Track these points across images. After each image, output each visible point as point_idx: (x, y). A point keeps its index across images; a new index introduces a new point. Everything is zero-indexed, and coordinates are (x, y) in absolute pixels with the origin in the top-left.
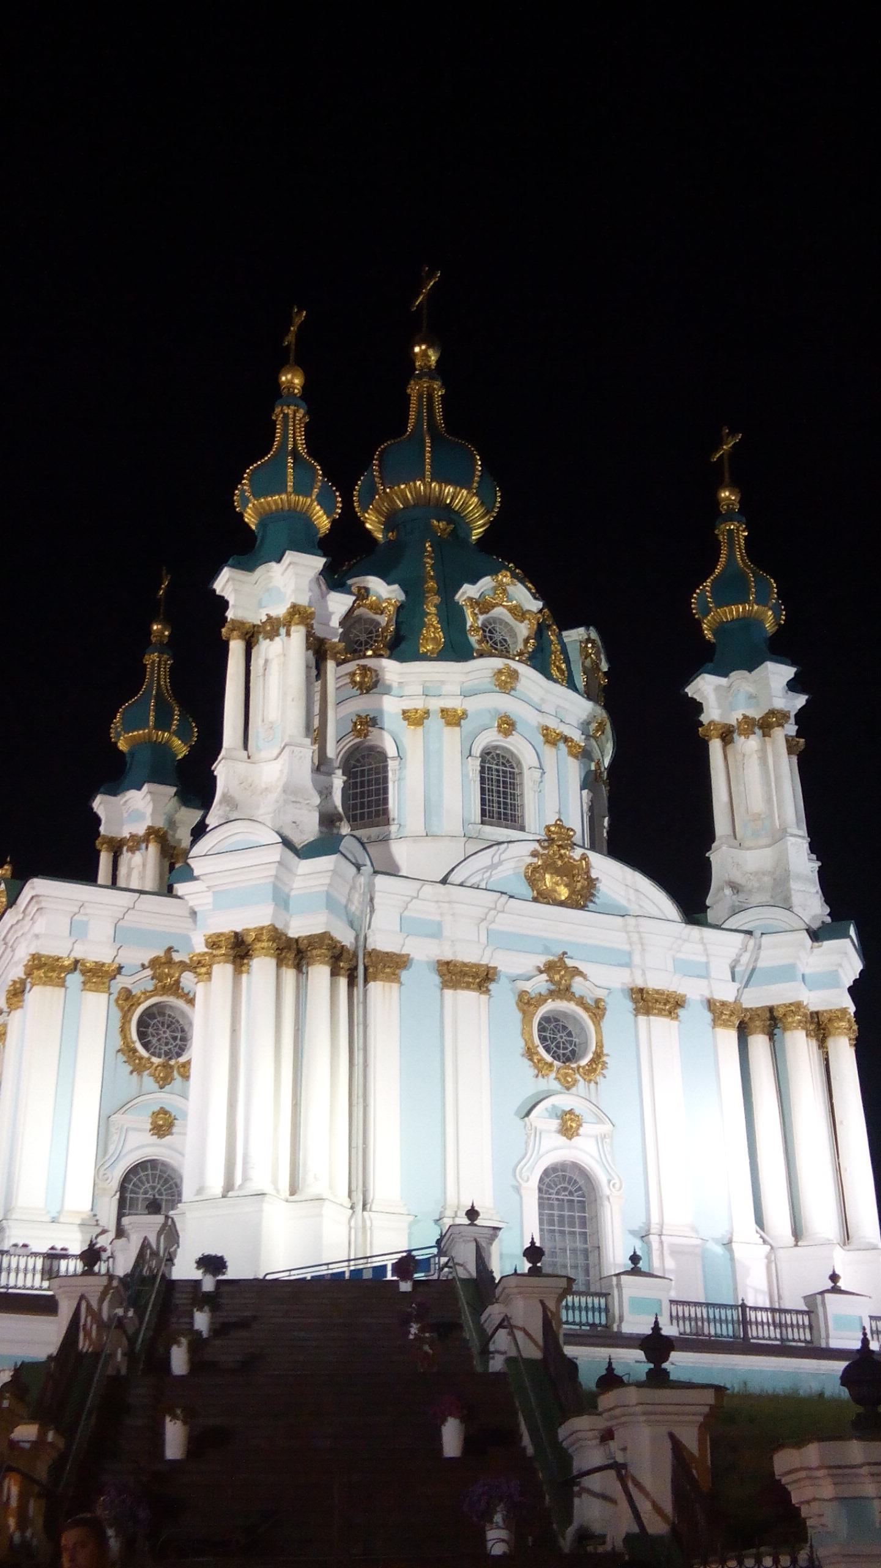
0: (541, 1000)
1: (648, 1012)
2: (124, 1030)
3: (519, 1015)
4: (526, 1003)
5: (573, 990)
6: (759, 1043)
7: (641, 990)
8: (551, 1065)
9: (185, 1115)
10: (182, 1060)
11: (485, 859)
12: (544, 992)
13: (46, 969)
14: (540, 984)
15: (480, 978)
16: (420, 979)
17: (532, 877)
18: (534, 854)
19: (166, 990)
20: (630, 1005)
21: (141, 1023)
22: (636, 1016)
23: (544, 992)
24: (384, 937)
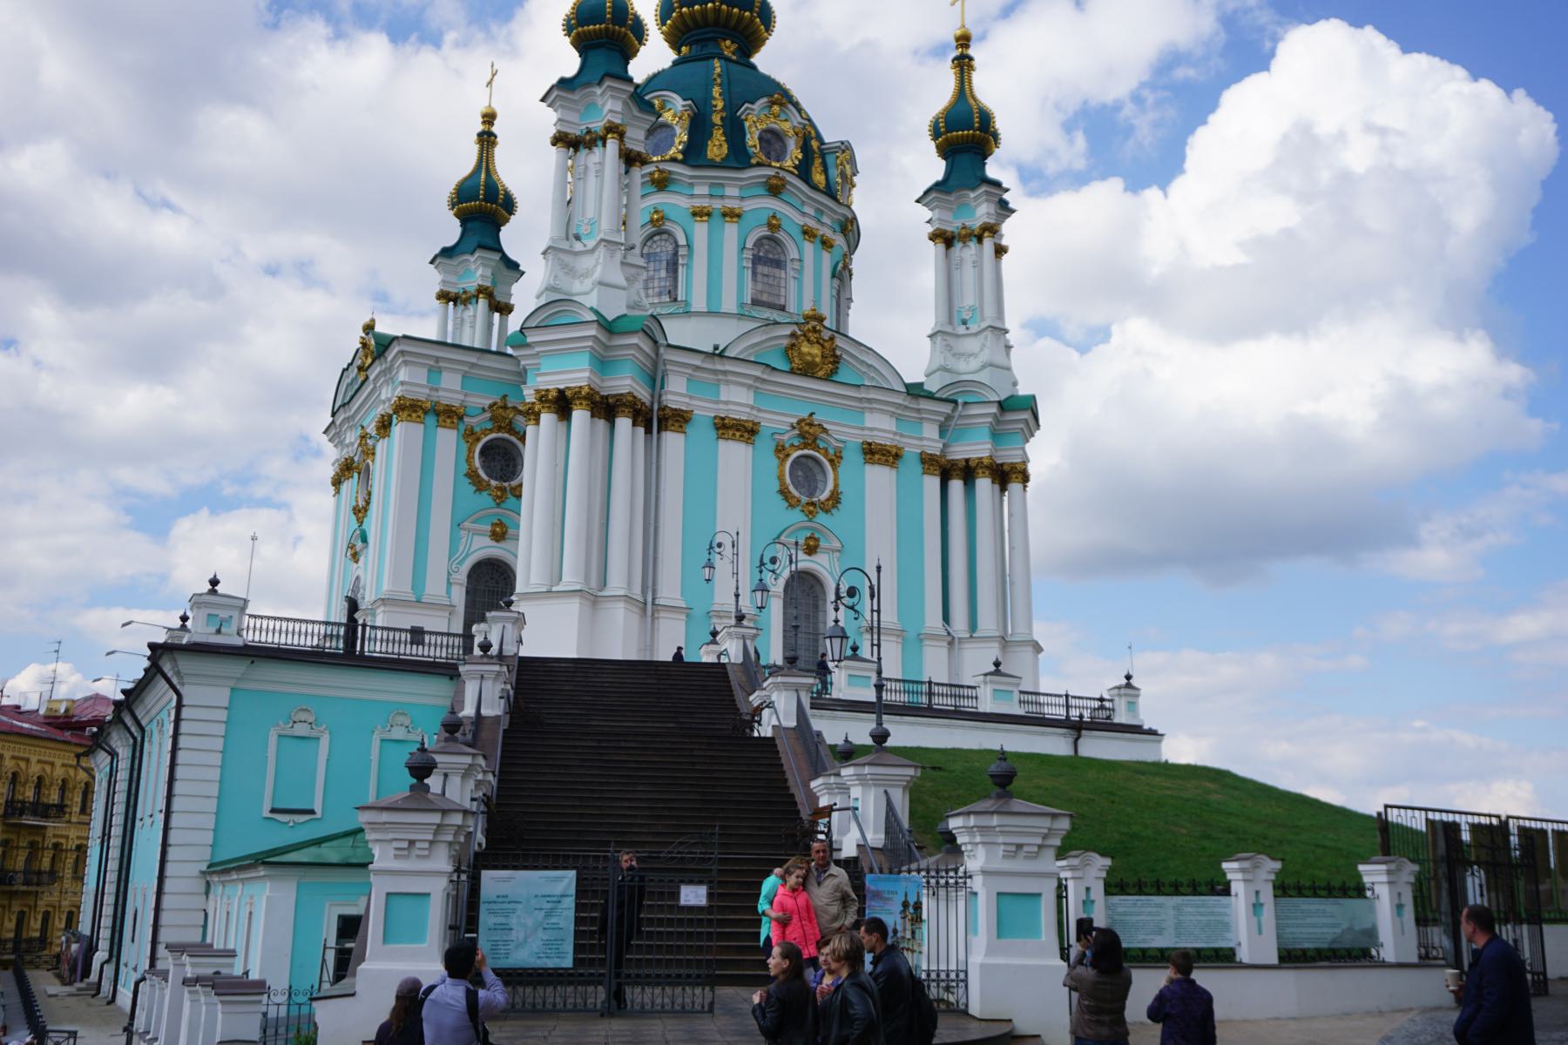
2: (469, 459)
3: (776, 462)
4: (781, 451)
10: (514, 483)
13: (408, 408)
15: (745, 431)
16: (701, 430)
17: (790, 350)
18: (793, 335)
19: (500, 429)
21: (482, 452)
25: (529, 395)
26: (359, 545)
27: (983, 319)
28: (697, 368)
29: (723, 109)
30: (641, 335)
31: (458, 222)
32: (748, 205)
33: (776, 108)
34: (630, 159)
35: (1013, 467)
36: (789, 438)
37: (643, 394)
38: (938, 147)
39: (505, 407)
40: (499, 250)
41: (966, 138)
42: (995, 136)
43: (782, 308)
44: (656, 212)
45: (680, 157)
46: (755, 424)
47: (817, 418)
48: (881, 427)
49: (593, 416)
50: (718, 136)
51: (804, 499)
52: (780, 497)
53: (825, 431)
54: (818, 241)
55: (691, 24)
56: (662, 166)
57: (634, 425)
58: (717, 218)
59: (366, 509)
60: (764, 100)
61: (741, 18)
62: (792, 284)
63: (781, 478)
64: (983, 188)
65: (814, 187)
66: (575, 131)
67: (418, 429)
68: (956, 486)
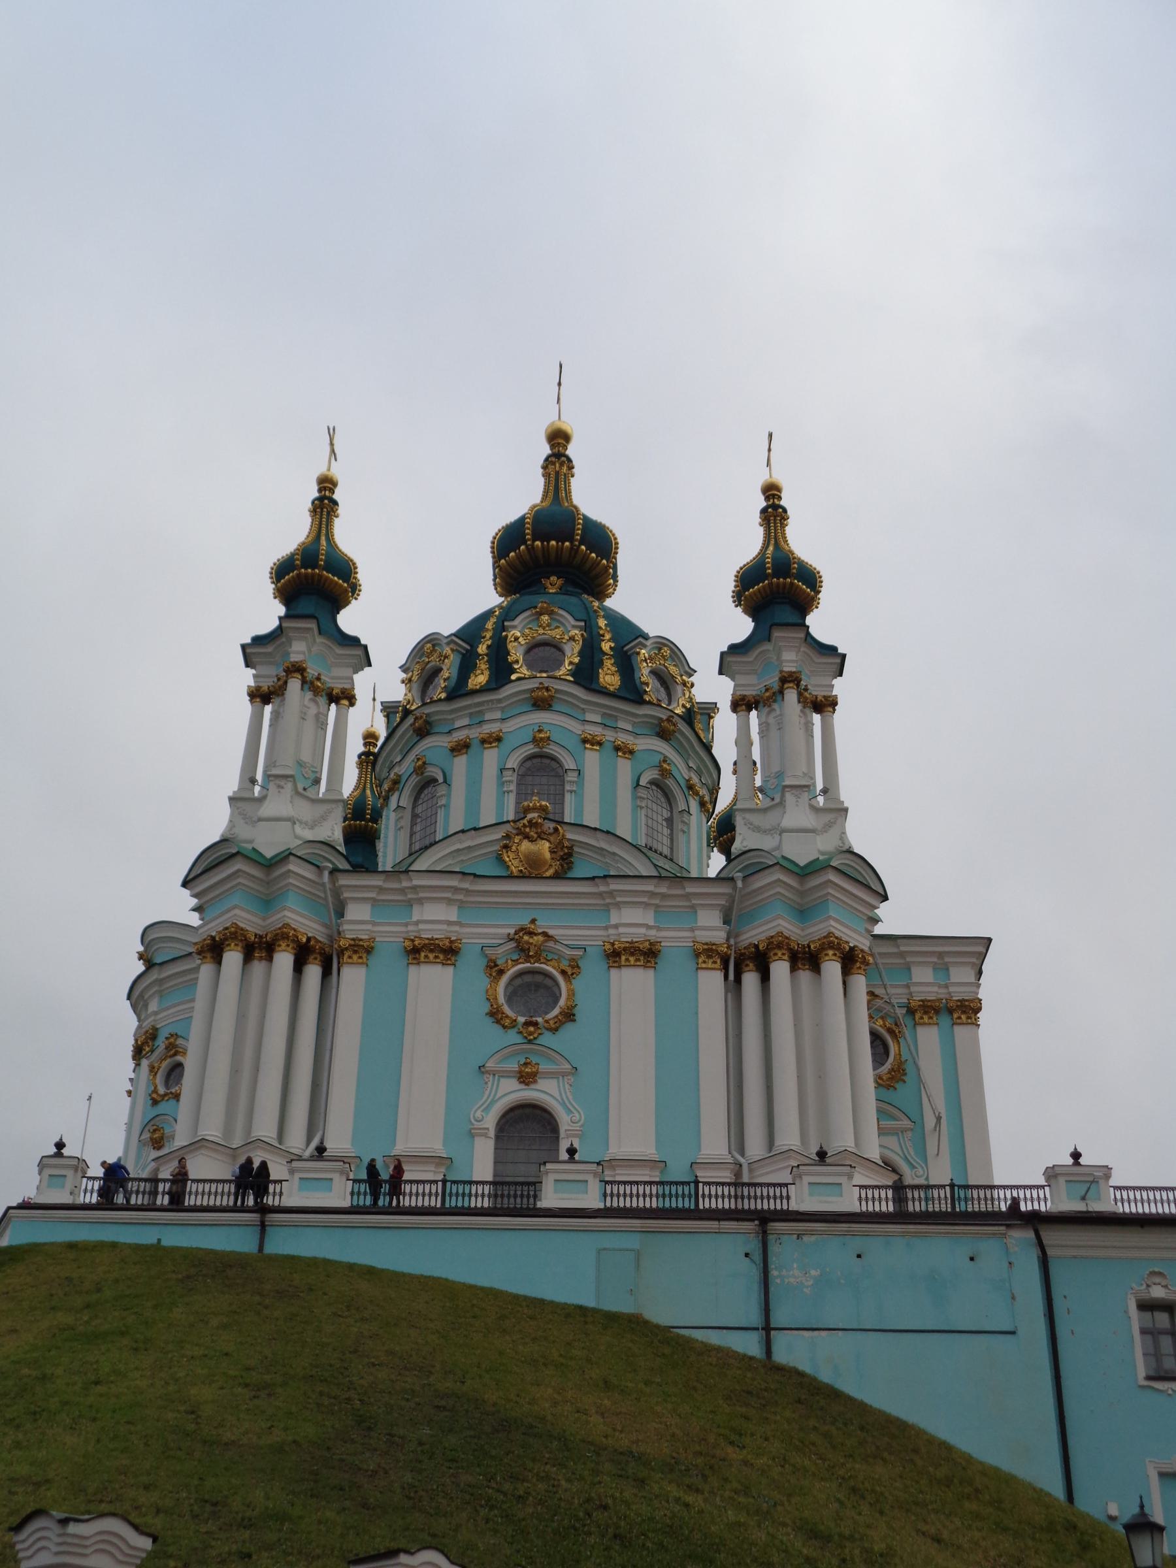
1: (620, 967)
4: (494, 969)
15: (447, 952)
28: (381, 889)
33: (545, 618)
36: (503, 952)
38: (745, 611)
41: (777, 590)
46: (451, 942)
48: (633, 922)
50: (483, 665)
52: (491, 1020)
54: (608, 747)
61: (559, 551)
63: (491, 999)
65: (604, 692)
68: (750, 980)
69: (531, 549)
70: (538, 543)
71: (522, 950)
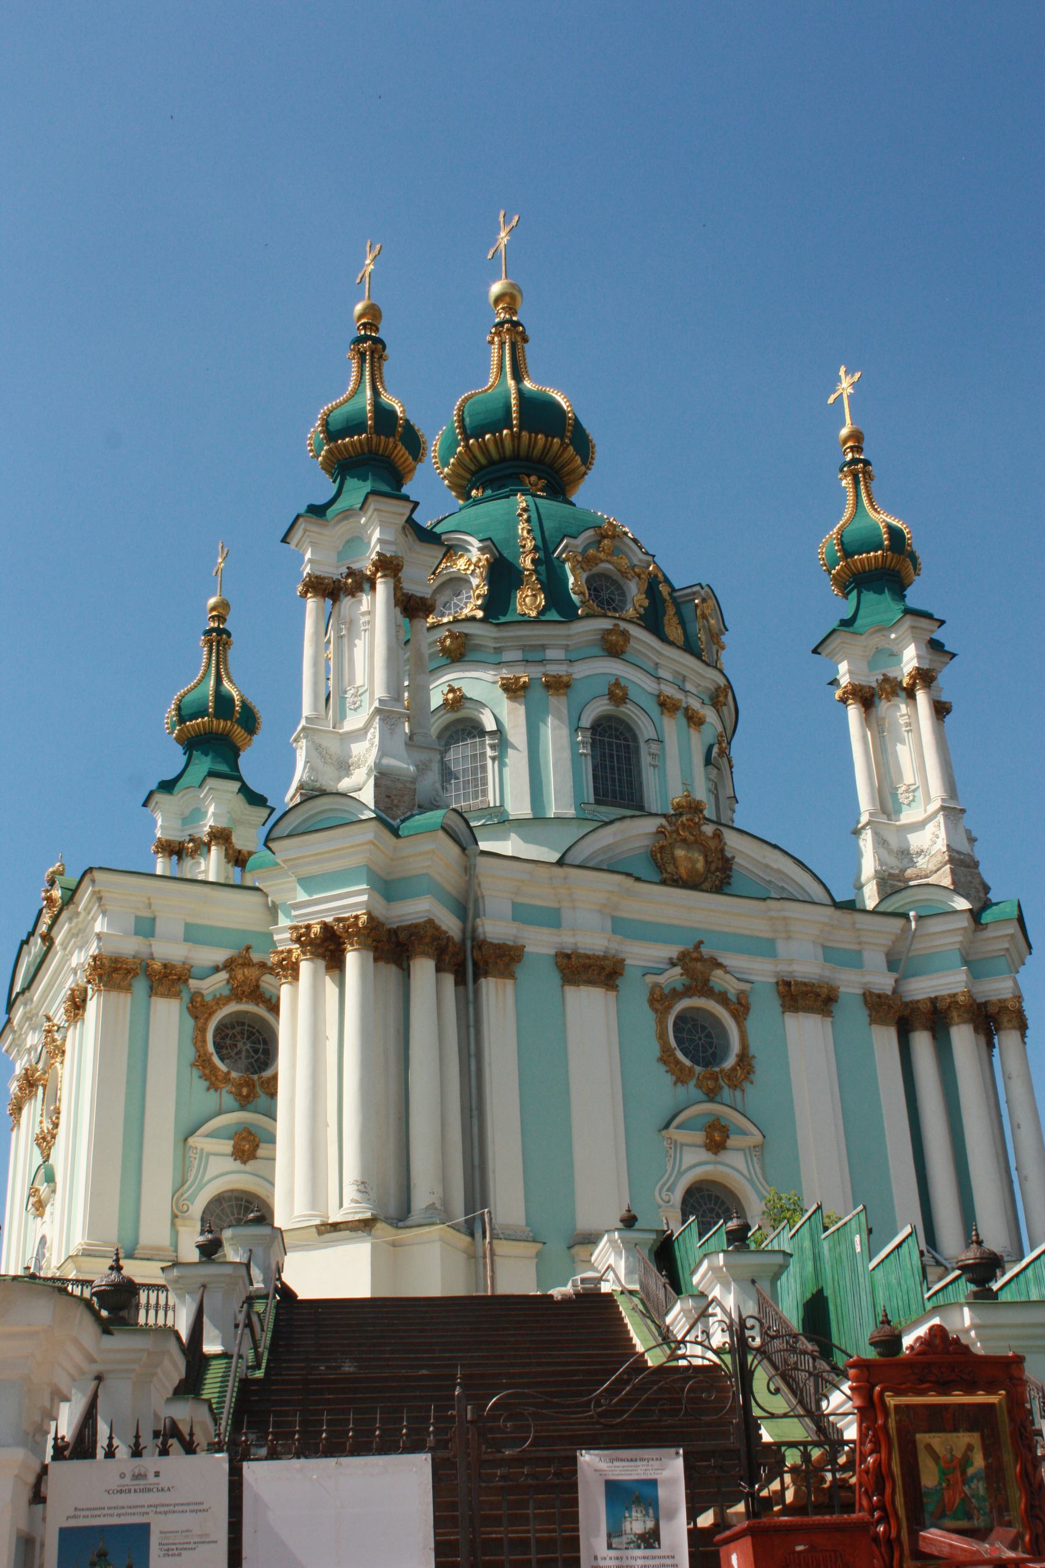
0: (676, 995)
2: (199, 1040)
4: (660, 1000)
5: (711, 984)
6: (922, 1043)
7: (788, 984)
8: (691, 1070)
9: (272, 1140)
11: (607, 837)
12: (679, 988)
13: (111, 972)
14: (674, 977)
18: (660, 832)
20: (776, 1003)
22: (783, 1013)
23: (679, 988)
24: (495, 928)
25: (283, 939)
26: (43, 1188)
27: (928, 799)
29: (536, 549)
30: (441, 834)
31: (180, 749)
32: (580, 671)
33: (606, 541)
34: (411, 607)
35: (1002, 1007)
37: (450, 924)
39: (248, 963)
40: (239, 778)
42: (913, 558)
43: (641, 808)
44: (452, 690)
45: (480, 614)
47: (705, 951)
49: (376, 960)
51: (698, 1069)
52: (663, 1068)
53: (720, 966)
54: (680, 715)
55: (483, 461)
56: (457, 629)
57: (438, 970)
58: (537, 693)
59: (54, 1137)
60: (591, 532)
62: (650, 779)
64: (909, 621)
65: (671, 644)
66: (333, 571)
67: (123, 1001)
69: (516, 437)
70: (524, 434)
71: (692, 978)
